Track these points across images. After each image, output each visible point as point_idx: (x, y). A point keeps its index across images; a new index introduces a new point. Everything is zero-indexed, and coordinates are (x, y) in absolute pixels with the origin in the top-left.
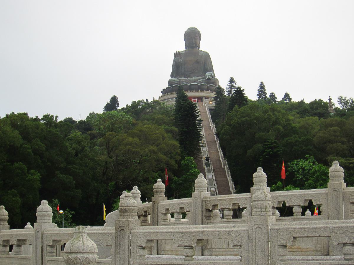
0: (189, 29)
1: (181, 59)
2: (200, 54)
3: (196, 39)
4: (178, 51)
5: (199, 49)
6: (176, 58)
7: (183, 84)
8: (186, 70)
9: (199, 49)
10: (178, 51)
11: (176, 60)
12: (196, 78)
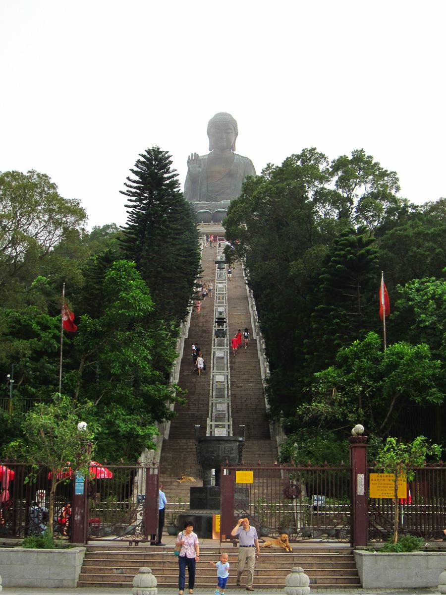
0: (216, 115)
1: (199, 167)
2: (235, 161)
3: (229, 133)
4: (195, 153)
5: (235, 152)
6: (191, 166)
7: (202, 211)
8: (210, 189)
9: (235, 152)
10: (195, 153)
11: (191, 169)
12: (226, 203)
